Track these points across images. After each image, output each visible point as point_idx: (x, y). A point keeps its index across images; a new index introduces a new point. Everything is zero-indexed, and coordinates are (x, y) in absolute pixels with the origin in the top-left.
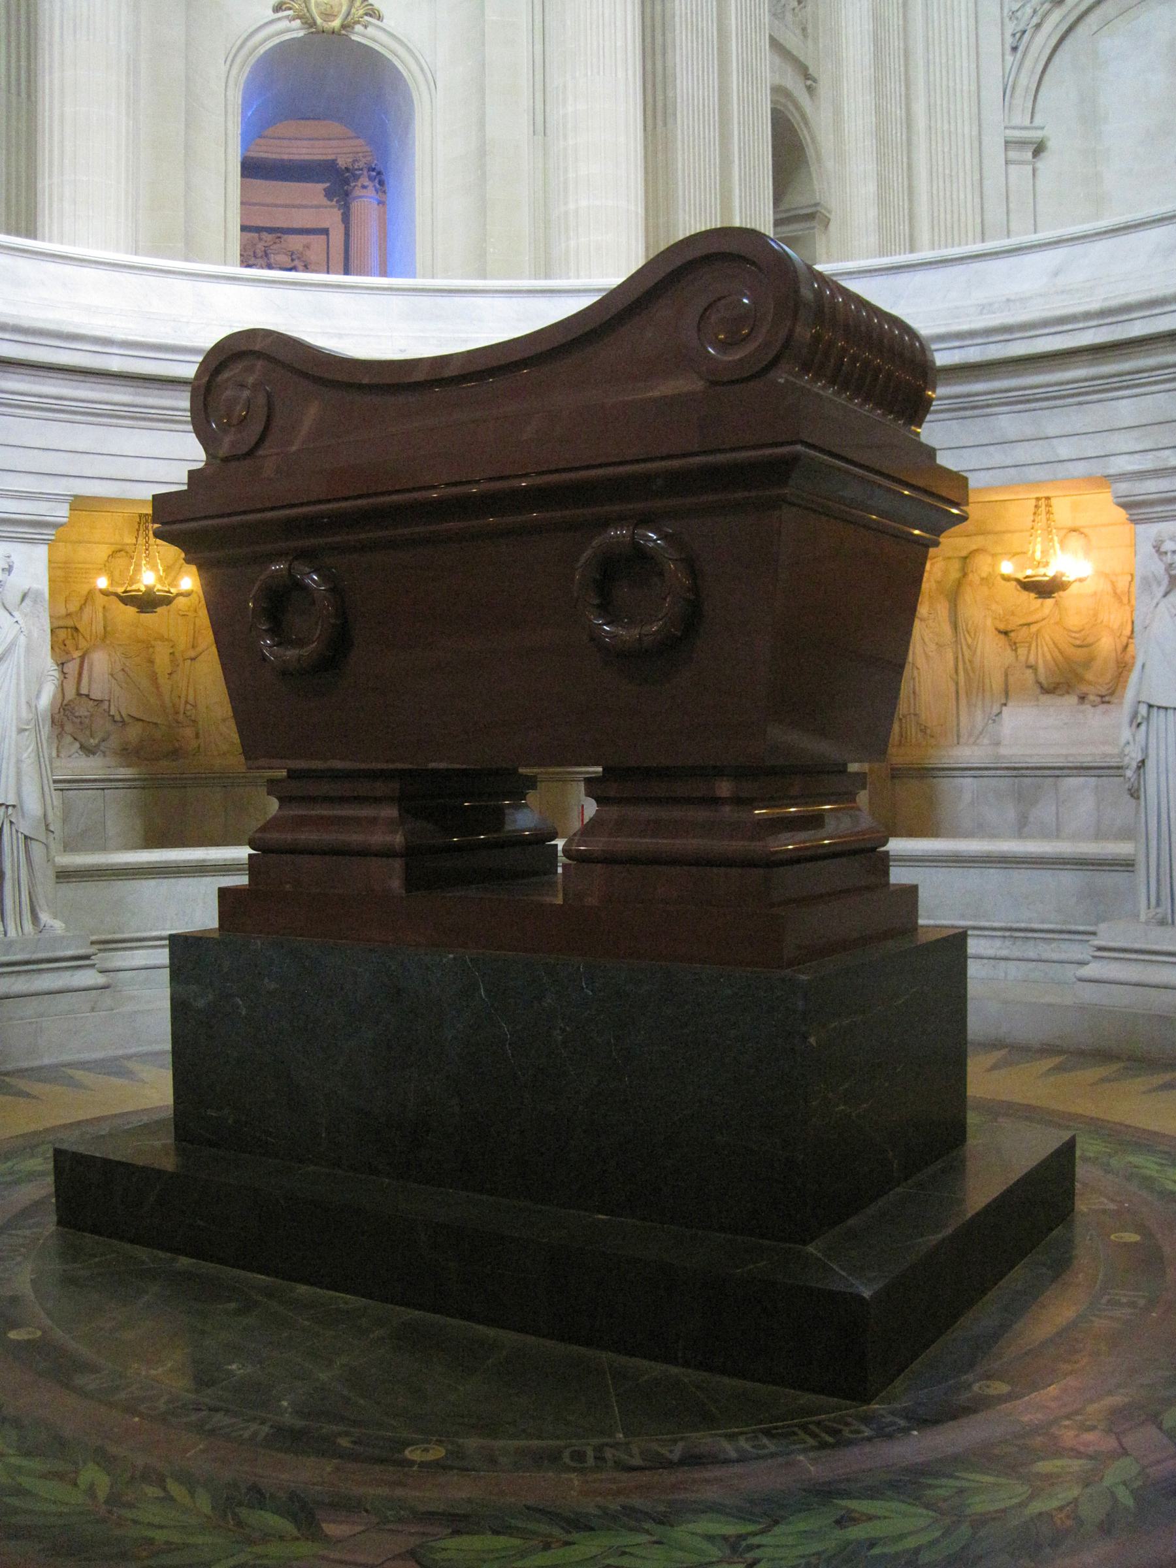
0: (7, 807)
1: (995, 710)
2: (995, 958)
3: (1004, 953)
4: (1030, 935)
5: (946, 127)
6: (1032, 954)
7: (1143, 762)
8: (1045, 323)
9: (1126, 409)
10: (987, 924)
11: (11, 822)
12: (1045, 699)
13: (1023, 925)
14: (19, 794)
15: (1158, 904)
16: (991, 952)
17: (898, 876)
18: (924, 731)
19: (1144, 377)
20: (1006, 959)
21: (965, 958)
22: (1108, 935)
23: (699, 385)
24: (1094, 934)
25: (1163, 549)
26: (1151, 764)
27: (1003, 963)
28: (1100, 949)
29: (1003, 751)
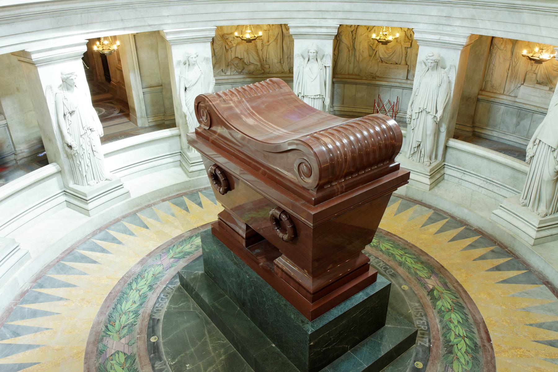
1: (519, 85)
3: (482, 185)
12: (537, 86)
15: (526, 199)
16: (479, 184)
26: (535, 158)
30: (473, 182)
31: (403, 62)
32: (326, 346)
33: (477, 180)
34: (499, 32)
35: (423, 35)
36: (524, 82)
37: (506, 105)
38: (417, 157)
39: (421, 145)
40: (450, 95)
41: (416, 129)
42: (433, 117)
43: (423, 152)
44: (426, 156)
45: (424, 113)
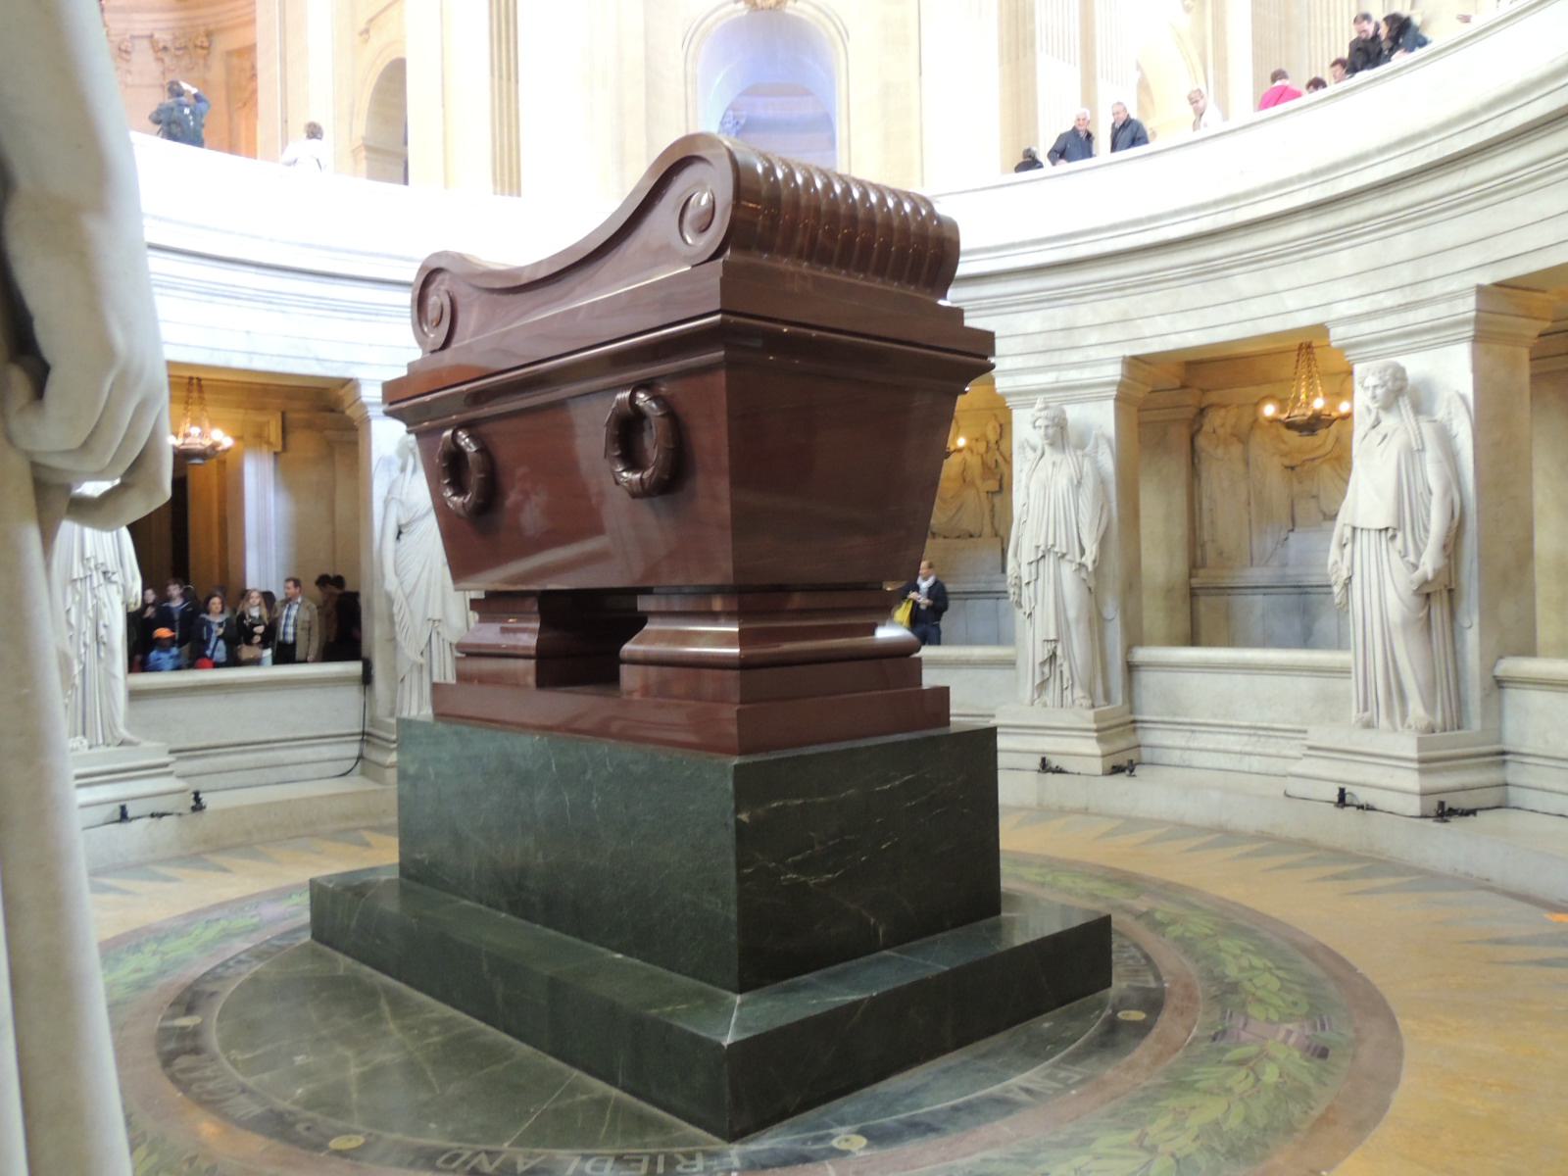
0: (434, 621)
1: (1283, 535)
2: (1241, 753)
3: (1248, 749)
4: (1271, 733)
5: (1325, 25)
6: (1272, 751)
7: (1350, 578)
8: (1265, 189)
9: (1345, 259)
10: (1234, 723)
11: (438, 633)
13: (1265, 725)
14: (444, 613)
15: (1366, 709)
16: (1238, 748)
17: (930, 679)
18: (1221, 554)
19: (1359, 229)
20: (1250, 754)
21: (996, 752)
22: (1319, 735)
23: (689, 268)
24: (1305, 732)
25: (1366, 384)
26: (1356, 580)
27: (1247, 757)
28: (1311, 748)
29: (1290, 571)
30: (1222, 747)
31: (987, 530)
32: (797, 867)
33: (1232, 738)
34: (1191, 335)
35: (1017, 378)
36: (1294, 525)
37: (1266, 589)
38: (1051, 694)
39: (1059, 652)
40: (1110, 510)
41: (1037, 614)
42: (1074, 567)
43: (1066, 674)
44: (1077, 684)
45: (1051, 559)
